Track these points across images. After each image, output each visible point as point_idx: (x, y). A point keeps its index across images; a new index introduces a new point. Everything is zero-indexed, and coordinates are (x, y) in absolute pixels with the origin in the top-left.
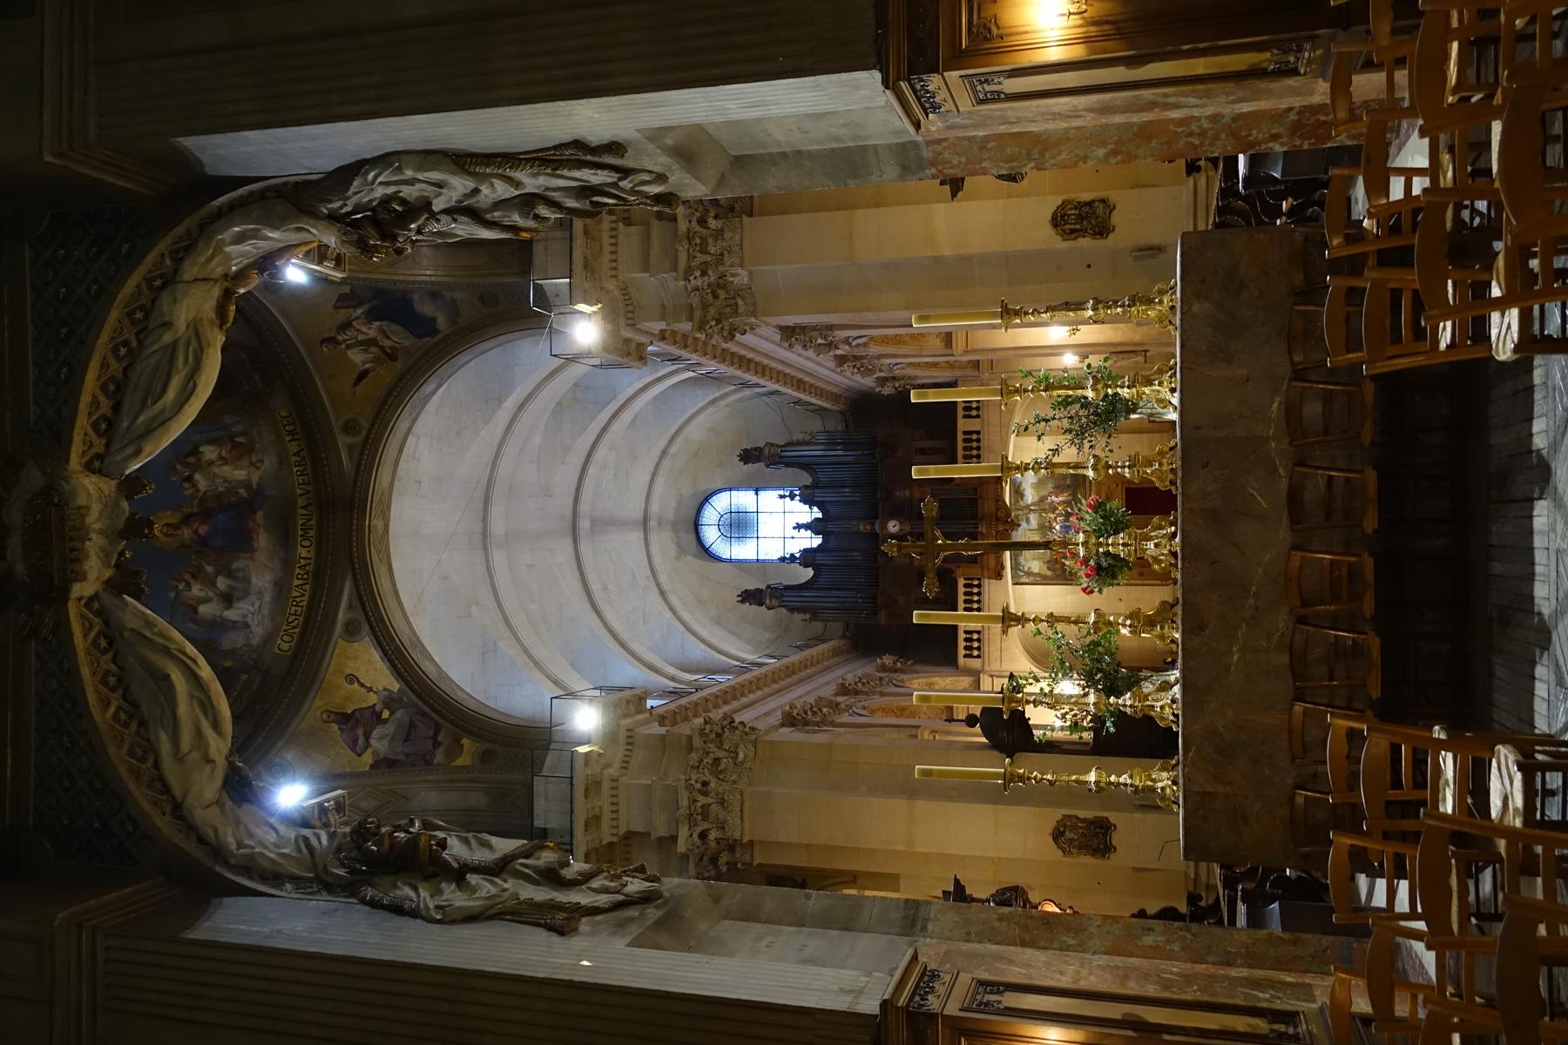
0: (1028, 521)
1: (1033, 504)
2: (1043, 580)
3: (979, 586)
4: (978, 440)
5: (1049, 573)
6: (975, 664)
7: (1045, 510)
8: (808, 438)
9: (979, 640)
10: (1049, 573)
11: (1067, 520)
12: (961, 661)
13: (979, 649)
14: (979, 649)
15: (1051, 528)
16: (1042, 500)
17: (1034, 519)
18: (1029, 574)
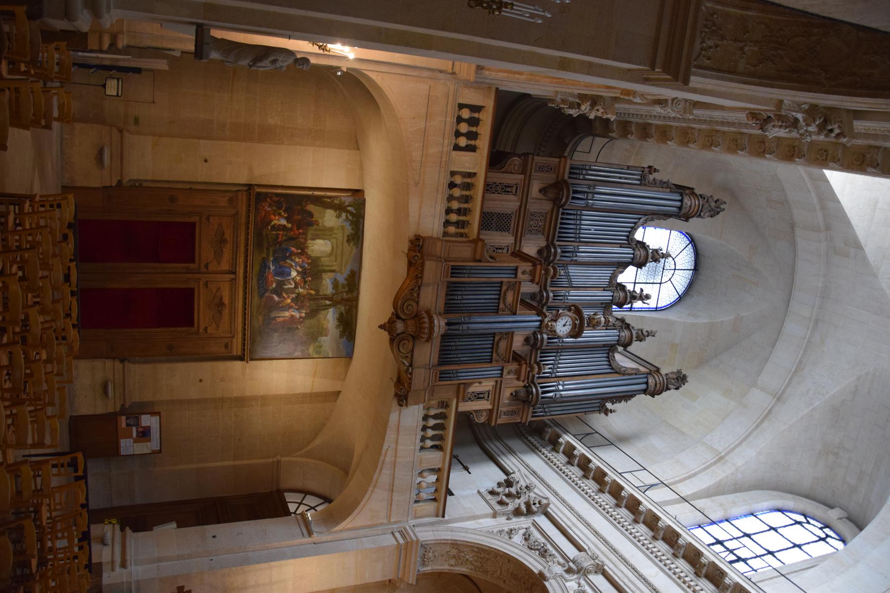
0: (335, 284)
1: (326, 307)
2: (321, 198)
3: (447, 223)
4: (423, 439)
5: (311, 208)
6: (472, 97)
7: (312, 298)
8: (609, 405)
9: (458, 134)
10: (311, 208)
11: (281, 284)
12: (489, 103)
13: (460, 120)
14: (460, 120)
15: (303, 273)
16: (313, 313)
17: (327, 285)
18: (340, 208)
